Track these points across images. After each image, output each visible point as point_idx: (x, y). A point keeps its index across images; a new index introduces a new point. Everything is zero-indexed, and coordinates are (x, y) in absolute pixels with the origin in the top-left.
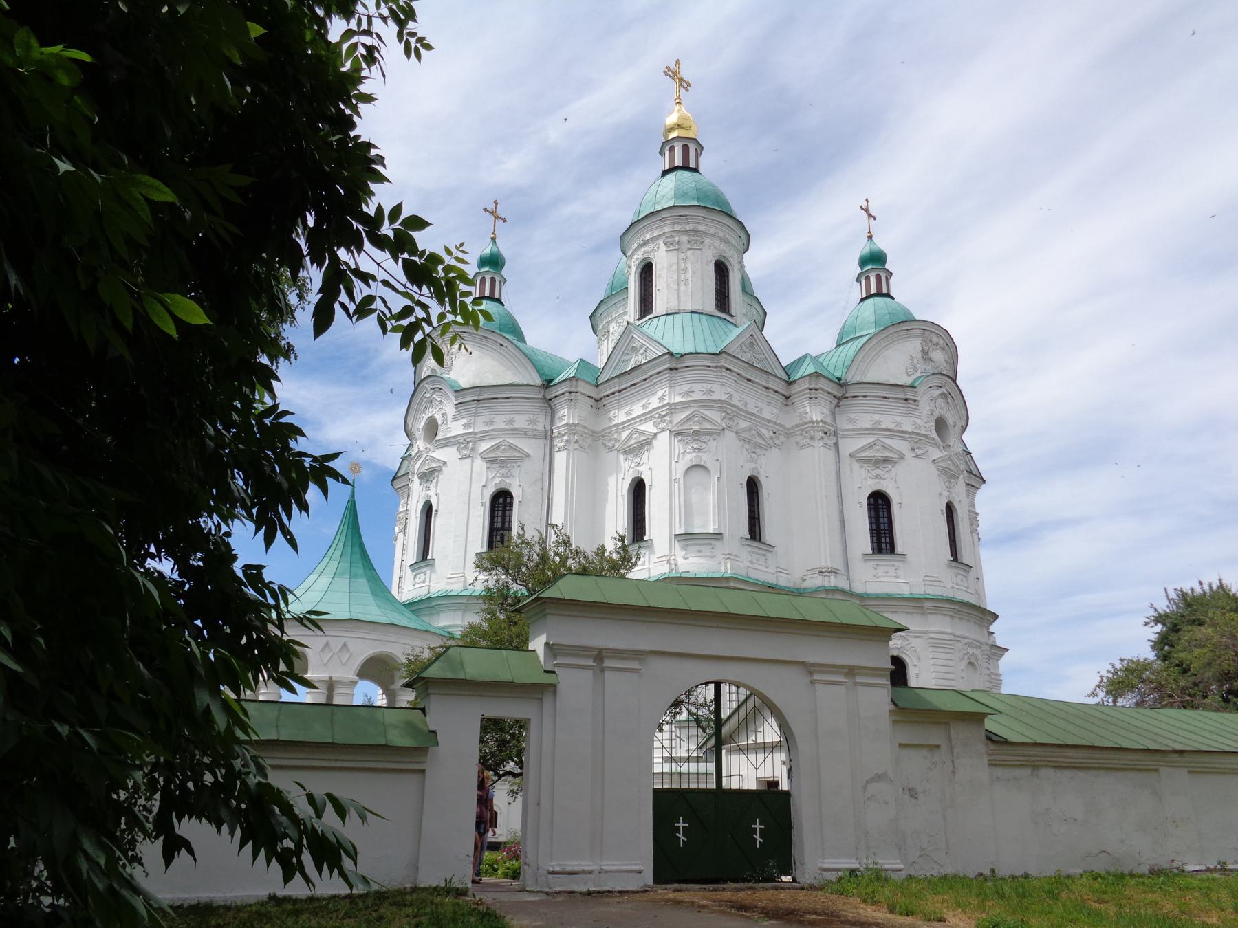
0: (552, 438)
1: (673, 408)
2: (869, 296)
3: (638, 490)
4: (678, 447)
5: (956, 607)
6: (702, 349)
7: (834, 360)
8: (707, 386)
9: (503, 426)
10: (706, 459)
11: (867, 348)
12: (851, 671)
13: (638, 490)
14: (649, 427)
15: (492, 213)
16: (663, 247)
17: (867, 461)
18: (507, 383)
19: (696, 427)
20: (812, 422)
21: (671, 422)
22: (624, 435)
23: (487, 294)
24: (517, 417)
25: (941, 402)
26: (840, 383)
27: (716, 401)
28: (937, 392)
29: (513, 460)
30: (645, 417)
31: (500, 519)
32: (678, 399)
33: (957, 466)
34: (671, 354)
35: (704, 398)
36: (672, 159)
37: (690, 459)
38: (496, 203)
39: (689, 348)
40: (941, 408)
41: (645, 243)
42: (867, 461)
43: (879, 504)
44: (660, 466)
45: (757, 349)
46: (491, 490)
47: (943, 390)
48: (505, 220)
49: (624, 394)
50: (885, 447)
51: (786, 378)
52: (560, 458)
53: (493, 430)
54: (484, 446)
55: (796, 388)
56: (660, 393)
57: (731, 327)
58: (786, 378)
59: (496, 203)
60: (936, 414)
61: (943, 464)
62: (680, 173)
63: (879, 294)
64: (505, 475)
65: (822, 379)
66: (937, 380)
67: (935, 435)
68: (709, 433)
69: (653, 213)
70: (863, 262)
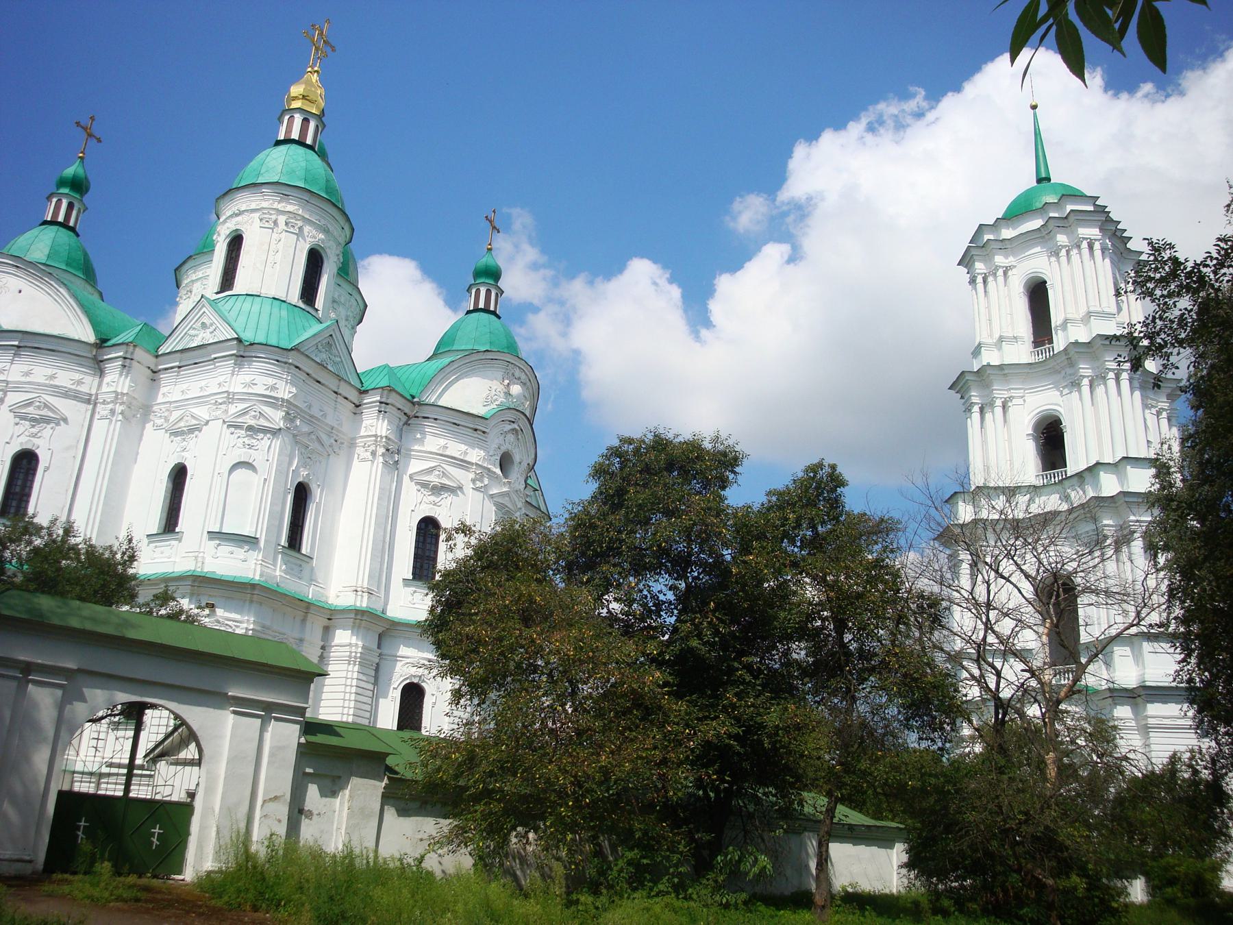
0: (95, 404)
1: (230, 398)
2: (476, 310)
3: (179, 475)
6: (273, 342)
7: (414, 375)
8: (271, 381)
9: (42, 380)
10: (257, 457)
11: (448, 369)
12: (269, 708)
13: (179, 475)
14: (203, 412)
15: (85, 129)
16: (257, 223)
17: (424, 485)
18: (55, 333)
19: (252, 422)
20: (376, 436)
21: (226, 411)
22: (176, 415)
23: (61, 219)
24: (60, 373)
25: (511, 437)
26: (411, 400)
28: (508, 427)
29: (46, 420)
30: (200, 400)
31: (19, 482)
32: (239, 389)
34: (239, 340)
35: (267, 393)
36: (289, 130)
37: (241, 454)
38: (92, 118)
39: (260, 338)
40: (509, 443)
41: (240, 213)
42: (424, 485)
44: (207, 458)
45: (334, 351)
47: (515, 426)
48: (99, 141)
51: (359, 386)
52: (99, 426)
53: (29, 383)
55: (368, 399)
56: (221, 379)
57: (313, 321)
58: (359, 386)
59: (92, 118)
60: (504, 449)
62: (294, 147)
63: (486, 310)
64: (34, 436)
65: (394, 394)
67: (498, 471)
68: (265, 431)
69: (254, 185)
70: (478, 274)
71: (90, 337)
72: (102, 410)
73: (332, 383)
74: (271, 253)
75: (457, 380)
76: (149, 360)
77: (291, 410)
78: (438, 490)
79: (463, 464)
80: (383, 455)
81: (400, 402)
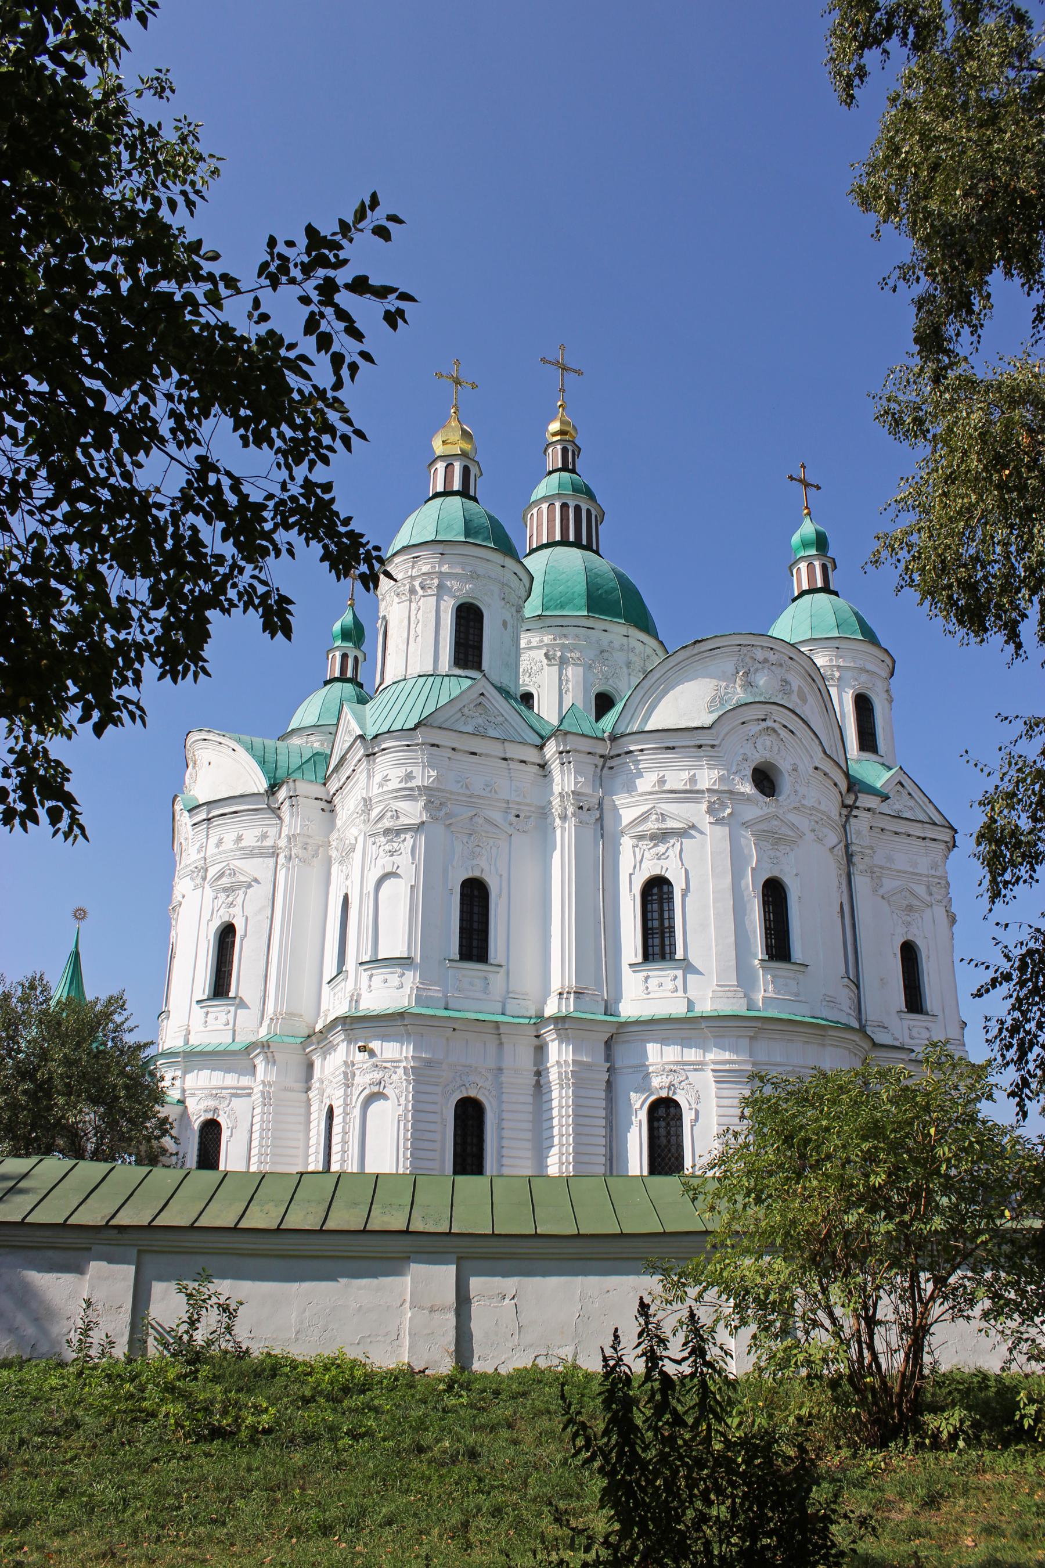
4: (372, 850)
5: (759, 1025)
16: (396, 599)
25: (767, 740)
27: (411, 789)
33: (793, 826)
37: (384, 864)
43: (656, 892)
46: (216, 924)
49: (345, 791)
50: (663, 817)
54: (212, 872)
61: (763, 826)
65: (570, 737)
66: (759, 711)
72: (281, 859)
73: (497, 749)
74: (413, 626)
75: (665, 692)
76: (318, 790)
77: (435, 799)
78: (661, 836)
79: (690, 794)
80: (574, 815)
81: (585, 745)
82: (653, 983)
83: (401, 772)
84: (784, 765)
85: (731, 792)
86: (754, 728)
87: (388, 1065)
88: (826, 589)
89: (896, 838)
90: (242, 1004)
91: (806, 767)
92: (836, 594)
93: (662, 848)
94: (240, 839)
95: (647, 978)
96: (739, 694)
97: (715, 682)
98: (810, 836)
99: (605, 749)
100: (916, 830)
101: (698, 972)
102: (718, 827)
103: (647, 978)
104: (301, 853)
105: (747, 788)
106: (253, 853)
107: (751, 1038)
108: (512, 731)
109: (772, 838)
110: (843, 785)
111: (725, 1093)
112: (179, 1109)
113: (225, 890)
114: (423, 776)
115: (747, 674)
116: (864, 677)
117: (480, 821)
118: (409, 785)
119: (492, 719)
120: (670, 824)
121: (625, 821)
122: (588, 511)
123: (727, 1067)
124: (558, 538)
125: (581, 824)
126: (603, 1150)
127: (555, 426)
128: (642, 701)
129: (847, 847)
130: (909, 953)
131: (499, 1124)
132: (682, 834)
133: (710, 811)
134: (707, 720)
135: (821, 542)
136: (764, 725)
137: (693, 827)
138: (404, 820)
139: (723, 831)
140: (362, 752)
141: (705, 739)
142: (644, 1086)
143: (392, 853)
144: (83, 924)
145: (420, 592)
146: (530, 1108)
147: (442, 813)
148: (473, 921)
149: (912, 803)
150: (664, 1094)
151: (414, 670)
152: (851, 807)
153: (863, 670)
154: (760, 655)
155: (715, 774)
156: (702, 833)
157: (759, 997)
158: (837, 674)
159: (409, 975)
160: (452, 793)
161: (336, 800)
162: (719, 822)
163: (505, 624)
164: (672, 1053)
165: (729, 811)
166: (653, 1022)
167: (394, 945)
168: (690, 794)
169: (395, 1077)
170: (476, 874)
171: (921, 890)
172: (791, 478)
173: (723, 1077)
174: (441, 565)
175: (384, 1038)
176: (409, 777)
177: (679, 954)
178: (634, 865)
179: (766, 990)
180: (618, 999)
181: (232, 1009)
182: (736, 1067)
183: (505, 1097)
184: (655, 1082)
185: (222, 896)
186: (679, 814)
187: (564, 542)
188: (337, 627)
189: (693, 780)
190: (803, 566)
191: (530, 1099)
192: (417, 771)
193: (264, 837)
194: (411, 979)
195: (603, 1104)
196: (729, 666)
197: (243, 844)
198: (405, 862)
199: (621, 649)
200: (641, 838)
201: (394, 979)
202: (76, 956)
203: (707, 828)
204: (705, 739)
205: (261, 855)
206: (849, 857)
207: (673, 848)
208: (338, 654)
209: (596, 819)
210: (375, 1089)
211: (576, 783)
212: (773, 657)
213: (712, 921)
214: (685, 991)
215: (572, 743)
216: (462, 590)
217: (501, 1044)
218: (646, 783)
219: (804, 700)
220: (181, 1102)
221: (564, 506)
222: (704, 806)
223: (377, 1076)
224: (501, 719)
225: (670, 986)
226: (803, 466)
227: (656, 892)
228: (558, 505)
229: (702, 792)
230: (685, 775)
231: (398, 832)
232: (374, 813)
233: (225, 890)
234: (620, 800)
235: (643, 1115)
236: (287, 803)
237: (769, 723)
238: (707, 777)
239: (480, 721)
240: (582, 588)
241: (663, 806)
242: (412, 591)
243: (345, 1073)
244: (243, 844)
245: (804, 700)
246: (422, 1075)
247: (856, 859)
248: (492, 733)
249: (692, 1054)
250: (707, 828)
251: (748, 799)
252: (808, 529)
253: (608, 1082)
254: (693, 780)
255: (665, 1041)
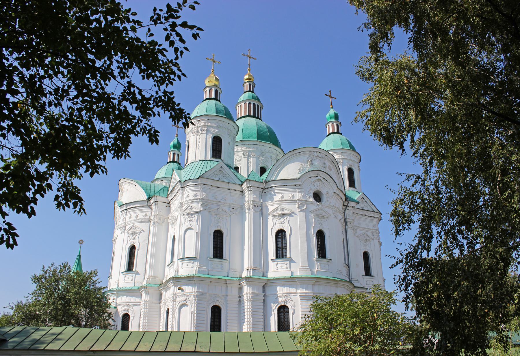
4: (183, 220)
5: (315, 280)
16: (192, 135)
25: (318, 183)
27: (197, 199)
28: (314, 179)
33: (327, 212)
37: (187, 225)
43: (280, 234)
46: (129, 245)
50: (283, 209)
61: (317, 212)
65: (251, 182)
66: (316, 173)
71: (145, 198)
72: (152, 223)
73: (226, 186)
74: (198, 144)
75: (284, 167)
76: (165, 200)
77: (205, 202)
78: (282, 216)
79: (292, 201)
80: (252, 208)
81: (257, 185)
82: (279, 266)
83: (193, 193)
84: (324, 191)
85: (306, 201)
86: (314, 179)
87: (188, 294)
88: (338, 132)
89: (361, 216)
90: (137, 273)
91: (331, 192)
92: (341, 134)
93: (282, 220)
94: (137, 216)
95: (277, 264)
96: (309, 168)
97: (300, 163)
98: (333, 216)
99: (263, 186)
100: (368, 214)
101: (295, 262)
102: (301, 213)
103: (277, 264)
104: (159, 221)
105: (312, 199)
106: (142, 221)
107: (313, 285)
108: (231, 180)
109: (320, 217)
110: (344, 199)
111: (304, 303)
112: (115, 309)
113: (132, 234)
114: (201, 195)
115: (311, 161)
116: (351, 162)
117: (220, 210)
118: (196, 198)
119: (225, 175)
120: (285, 212)
121: (270, 211)
122: (258, 105)
123: (304, 295)
124: (247, 114)
125: (255, 211)
126: (262, 323)
127: (247, 77)
128: (276, 170)
129: (345, 220)
130: (366, 255)
131: (226, 314)
132: (289, 215)
133: (299, 207)
134: (298, 176)
135: (336, 117)
136: (317, 178)
137: (293, 212)
138: (194, 210)
139: (303, 214)
140: (180, 186)
141: (297, 183)
142: (276, 302)
143: (190, 221)
144: (82, 245)
145: (201, 132)
146: (237, 309)
147: (207, 208)
148: (218, 245)
149: (367, 205)
150: (283, 304)
151: (198, 159)
152: (346, 206)
153: (350, 160)
154: (316, 154)
155: (301, 195)
156: (296, 215)
157: (315, 270)
158: (342, 161)
159: (196, 263)
160: (211, 201)
161: (171, 203)
162: (302, 211)
163: (229, 143)
164: (286, 290)
165: (305, 207)
166: (279, 279)
167: (190, 252)
168: (292, 201)
169: (190, 298)
170: (219, 228)
171: (370, 234)
172: (326, 95)
173: (303, 298)
174: (208, 123)
175: (187, 285)
176: (196, 195)
177: (288, 256)
178: (273, 226)
179: (318, 268)
180: (267, 271)
181: (134, 275)
182: (307, 294)
183: (228, 305)
184: (280, 300)
185: (131, 236)
186: (288, 208)
187: (250, 116)
188: (172, 144)
189: (293, 196)
190: (330, 124)
191: (237, 306)
192: (199, 193)
193: (146, 215)
194: (196, 264)
195: (262, 307)
196: (305, 158)
197: (139, 218)
198: (194, 224)
199: (269, 152)
200: (275, 216)
201: (190, 265)
202: (79, 257)
203: (298, 213)
204: (297, 183)
205: (145, 222)
206: (346, 223)
207: (286, 219)
208: (172, 153)
209: (260, 210)
210: (184, 302)
211: (253, 198)
212: (320, 155)
213: (299, 245)
214: (290, 269)
215: (252, 184)
216: (215, 132)
217: (227, 287)
218: (277, 197)
219: (331, 170)
220: (116, 307)
221: (250, 104)
222: (297, 206)
223: (184, 298)
224: (228, 175)
225: (285, 267)
226: (330, 91)
227: (280, 234)
228: (247, 103)
229: (296, 201)
230: (290, 195)
231: (192, 214)
232: (184, 207)
233: (132, 234)
234: (268, 203)
235: (276, 311)
236: (154, 204)
237: (319, 177)
238: (298, 196)
239: (220, 176)
240: (255, 131)
241: (283, 205)
242: (198, 132)
243: (173, 297)
244: (139, 218)
245: (331, 170)
246: (199, 297)
247: (348, 224)
248: (225, 180)
249: (293, 290)
250: (298, 213)
251: (312, 203)
252: (332, 112)
253: (264, 300)
254: (293, 196)
255: (283, 286)
